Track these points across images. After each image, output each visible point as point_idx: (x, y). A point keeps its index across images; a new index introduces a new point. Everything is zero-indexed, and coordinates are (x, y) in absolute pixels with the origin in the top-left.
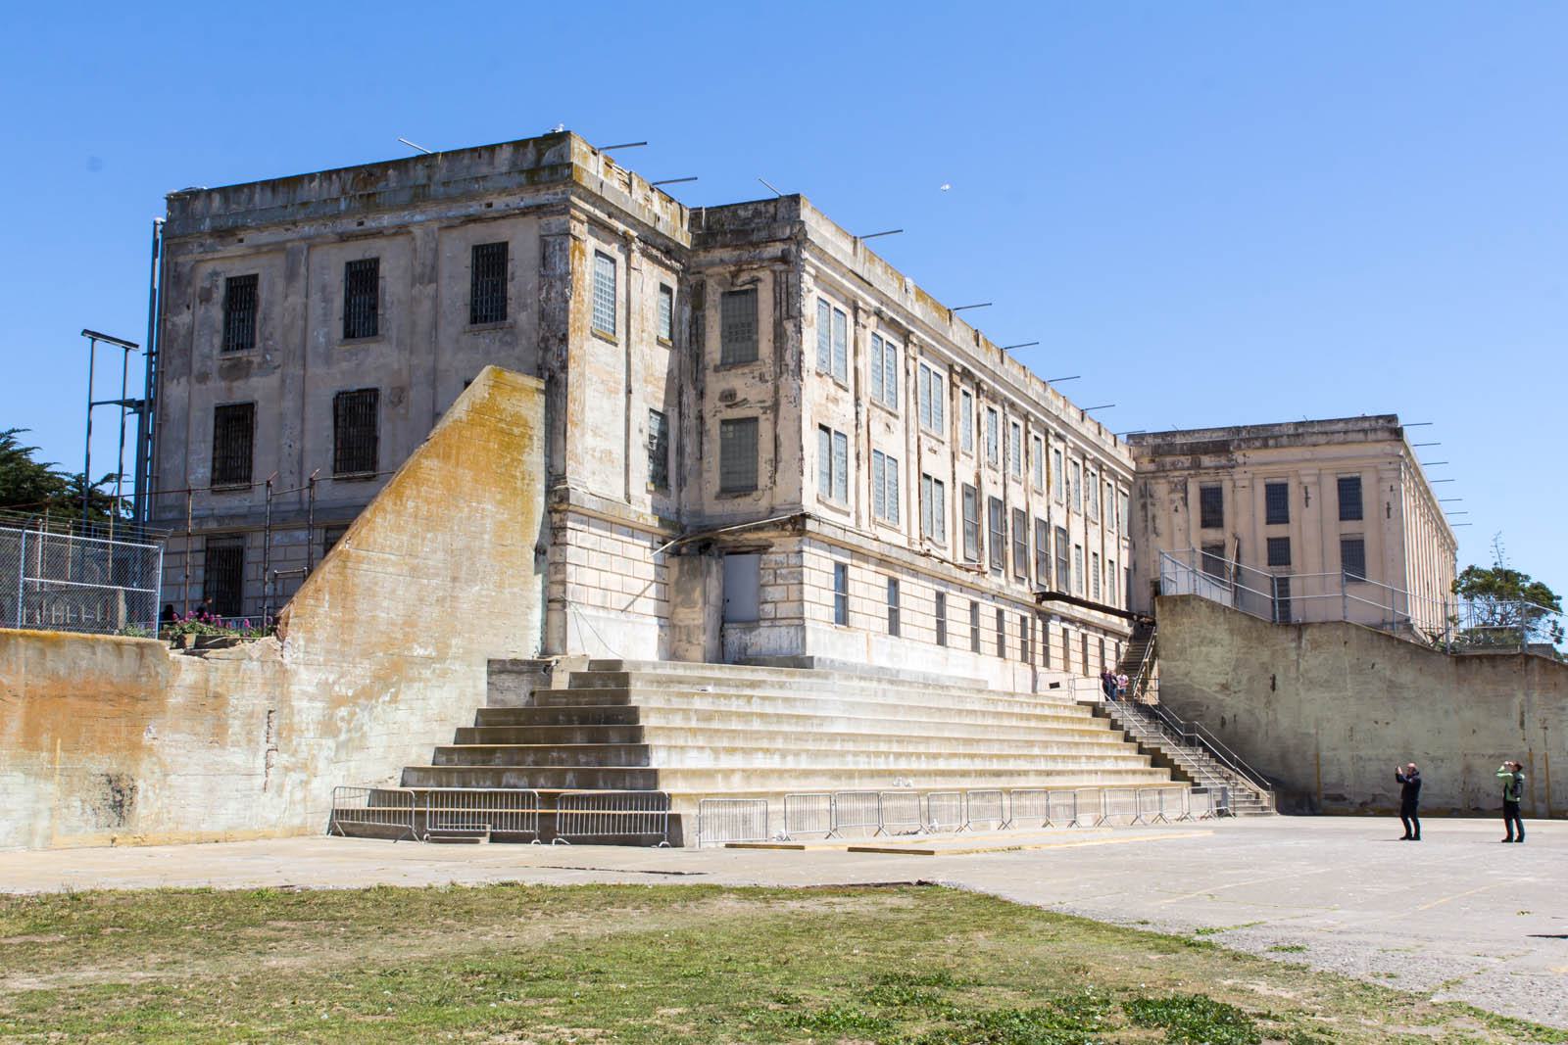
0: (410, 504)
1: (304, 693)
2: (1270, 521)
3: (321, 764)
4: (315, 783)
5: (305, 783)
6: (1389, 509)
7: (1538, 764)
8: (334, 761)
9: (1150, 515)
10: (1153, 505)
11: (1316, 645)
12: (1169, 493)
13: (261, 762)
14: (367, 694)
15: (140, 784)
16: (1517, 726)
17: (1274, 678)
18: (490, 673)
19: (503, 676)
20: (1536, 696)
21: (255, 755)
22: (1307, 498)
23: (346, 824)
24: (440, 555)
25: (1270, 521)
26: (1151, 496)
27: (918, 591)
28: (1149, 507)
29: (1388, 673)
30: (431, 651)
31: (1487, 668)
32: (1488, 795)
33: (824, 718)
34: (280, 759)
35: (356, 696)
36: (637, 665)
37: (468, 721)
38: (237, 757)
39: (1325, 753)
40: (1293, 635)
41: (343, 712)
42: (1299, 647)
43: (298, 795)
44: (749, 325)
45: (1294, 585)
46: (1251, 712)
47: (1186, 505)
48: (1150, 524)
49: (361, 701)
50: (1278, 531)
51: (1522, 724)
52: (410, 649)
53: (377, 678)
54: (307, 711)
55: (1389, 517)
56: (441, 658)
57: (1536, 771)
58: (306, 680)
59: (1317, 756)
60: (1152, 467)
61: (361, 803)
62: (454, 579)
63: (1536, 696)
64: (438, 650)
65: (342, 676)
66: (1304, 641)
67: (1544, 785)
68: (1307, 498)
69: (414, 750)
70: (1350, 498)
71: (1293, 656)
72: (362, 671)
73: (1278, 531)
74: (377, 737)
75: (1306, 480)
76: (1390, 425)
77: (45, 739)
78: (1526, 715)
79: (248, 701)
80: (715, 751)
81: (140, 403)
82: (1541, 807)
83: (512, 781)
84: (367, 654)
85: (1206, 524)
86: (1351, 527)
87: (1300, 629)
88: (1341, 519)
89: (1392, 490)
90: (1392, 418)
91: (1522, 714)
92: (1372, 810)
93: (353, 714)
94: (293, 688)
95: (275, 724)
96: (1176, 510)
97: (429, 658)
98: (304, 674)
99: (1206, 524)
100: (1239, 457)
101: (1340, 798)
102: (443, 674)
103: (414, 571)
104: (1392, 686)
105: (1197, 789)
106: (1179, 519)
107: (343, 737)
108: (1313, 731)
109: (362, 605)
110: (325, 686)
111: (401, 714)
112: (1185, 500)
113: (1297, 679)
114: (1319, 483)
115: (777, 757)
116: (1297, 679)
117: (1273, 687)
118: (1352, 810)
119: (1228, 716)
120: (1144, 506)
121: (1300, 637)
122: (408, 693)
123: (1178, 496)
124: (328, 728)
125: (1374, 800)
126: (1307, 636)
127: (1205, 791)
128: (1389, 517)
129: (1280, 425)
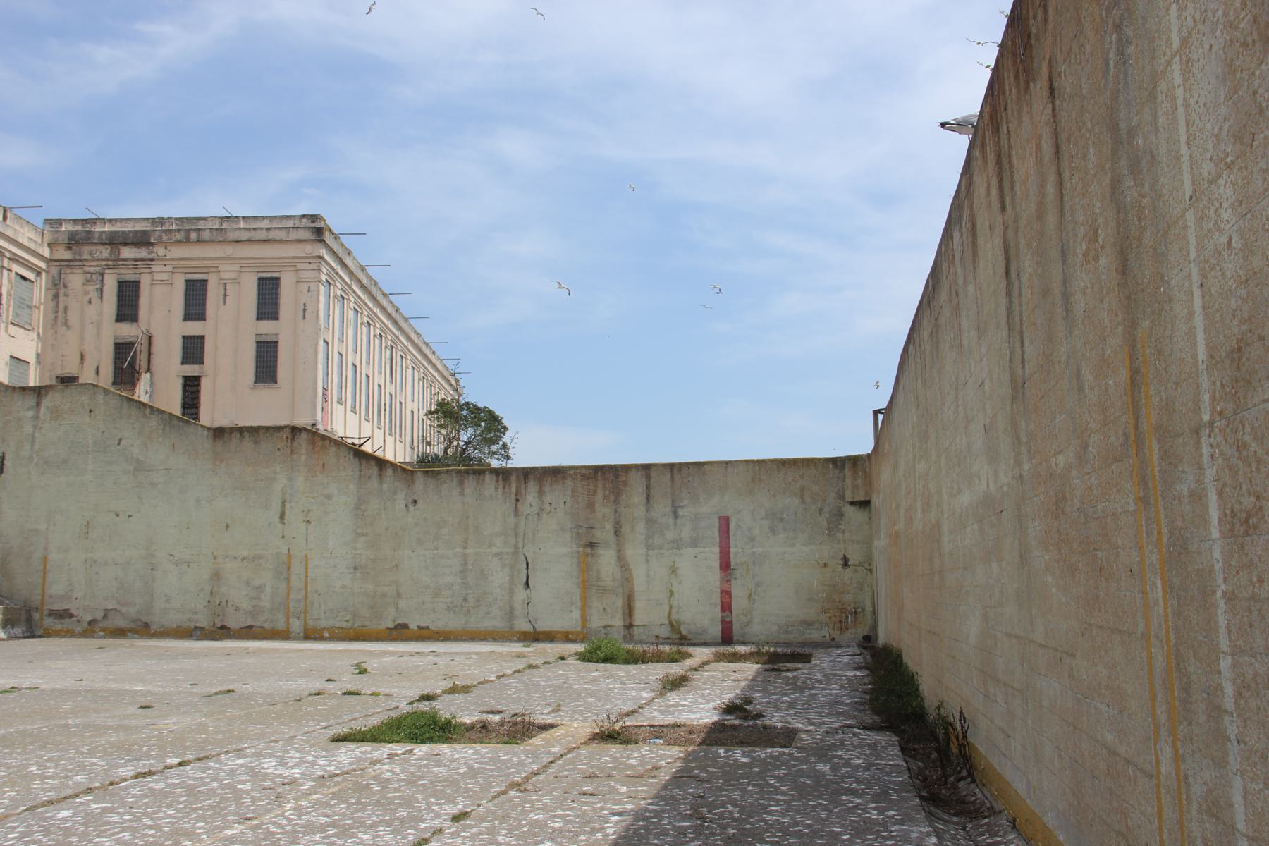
6: (305, 310)
7: (297, 568)
9: (61, 307)
10: (66, 295)
12: (84, 284)
16: (277, 519)
22: (225, 295)
26: (65, 286)
28: (62, 298)
29: (136, 451)
31: (247, 444)
32: (237, 609)
39: (53, 556)
40: (31, 401)
42: (36, 418)
45: (205, 385)
47: (101, 298)
48: (61, 315)
50: (194, 328)
51: (282, 517)
55: (304, 318)
57: (294, 578)
60: (68, 255)
63: (300, 480)
66: (43, 409)
67: (301, 596)
68: (225, 295)
71: (28, 428)
73: (194, 328)
75: (225, 276)
76: (313, 225)
78: (288, 505)
82: (296, 625)
85: (120, 318)
86: (267, 327)
87: (39, 395)
88: (258, 319)
89: (309, 291)
90: (314, 218)
91: (283, 503)
92: (103, 630)
96: (90, 302)
99: (120, 318)
100: (161, 251)
101: (65, 614)
104: (140, 467)
106: (91, 311)
108: (42, 527)
112: (101, 290)
113: (31, 458)
114: (237, 282)
116: (31, 458)
118: (78, 629)
120: (56, 296)
121: (38, 404)
123: (92, 288)
125: (105, 617)
128: (304, 318)
129: (205, 219)
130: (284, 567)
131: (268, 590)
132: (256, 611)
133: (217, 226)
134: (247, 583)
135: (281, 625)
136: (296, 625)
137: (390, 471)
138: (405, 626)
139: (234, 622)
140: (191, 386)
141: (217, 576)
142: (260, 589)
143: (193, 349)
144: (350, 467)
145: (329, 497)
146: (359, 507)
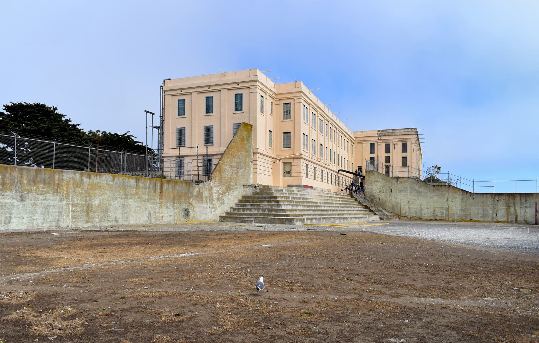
0: (231, 152)
1: (215, 192)
2: (386, 153)
3: (218, 207)
4: (217, 211)
5: (215, 211)
7: (450, 210)
8: (219, 206)
11: (401, 183)
13: (208, 206)
14: (224, 193)
15: (190, 211)
16: (446, 201)
17: (391, 190)
18: (244, 188)
19: (247, 189)
20: (451, 195)
21: (207, 205)
23: (223, 219)
24: (236, 163)
25: (386, 153)
27: (311, 167)
29: (417, 189)
30: (234, 184)
33: (307, 198)
34: (211, 206)
35: (223, 193)
36: (272, 187)
37: (240, 198)
38: (205, 205)
39: (402, 207)
40: (396, 180)
41: (221, 196)
43: (214, 213)
44: (289, 111)
46: (386, 197)
49: (224, 194)
51: (447, 201)
52: (231, 183)
53: (226, 189)
54: (215, 196)
56: (236, 185)
58: (215, 190)
59: (400, 207)
61: (224, 215)
62: (238, 168)
63: (451, 195)
64: (235, 183)
65: (220, 189)
67: (451, 214)
69: (232, 204)
70: (404, 148)
71: (396, 185)
72: (224, 188)
74: (226, 201)
77: (176, 202)
79: (206, 194)
80: (292, 206)
81: (159, 127)
82: (450, 219)
83: (254, 211)
84: (224, 184)
86: (404, 154)
90: (415, 128)
91: (447, 198)
93: (222, 197)
94: (213, 191)
95: (210, 199)
97: (234, 185)
98: (214, 189)
101: (405, 217)
102: (236, 188)
103: (232, 167)
104: (418, 192)
105: (375, 214)
107: (221, 201)
109: (223, 174)
110: (218, 191)
111: (230, 197)
113: (397, 190)
115: (313, 207)
116: (397, 190)
117: (391, 192)
119: (381, 198)
121: (398, 181)
122: (231, 192)
124: (218, 200)
125: (413, 217)
126: (399, 180)
127: (377, 215)
129: (389, 130)
130: (448, 209)
131: (445, 213)
132: (442, 217)
133: (392, 132)
134: (440, 212)
135: (447, 219)
136: (450, 219)
137: (468, 193)
138: (472, 220)
139: (438, 218)
140: (387, 168)
141: (434, 211)
142: (443, 213)
143: (388, 160)
144: (461, 193)
145: (456, 198)
146: (462, 200)
